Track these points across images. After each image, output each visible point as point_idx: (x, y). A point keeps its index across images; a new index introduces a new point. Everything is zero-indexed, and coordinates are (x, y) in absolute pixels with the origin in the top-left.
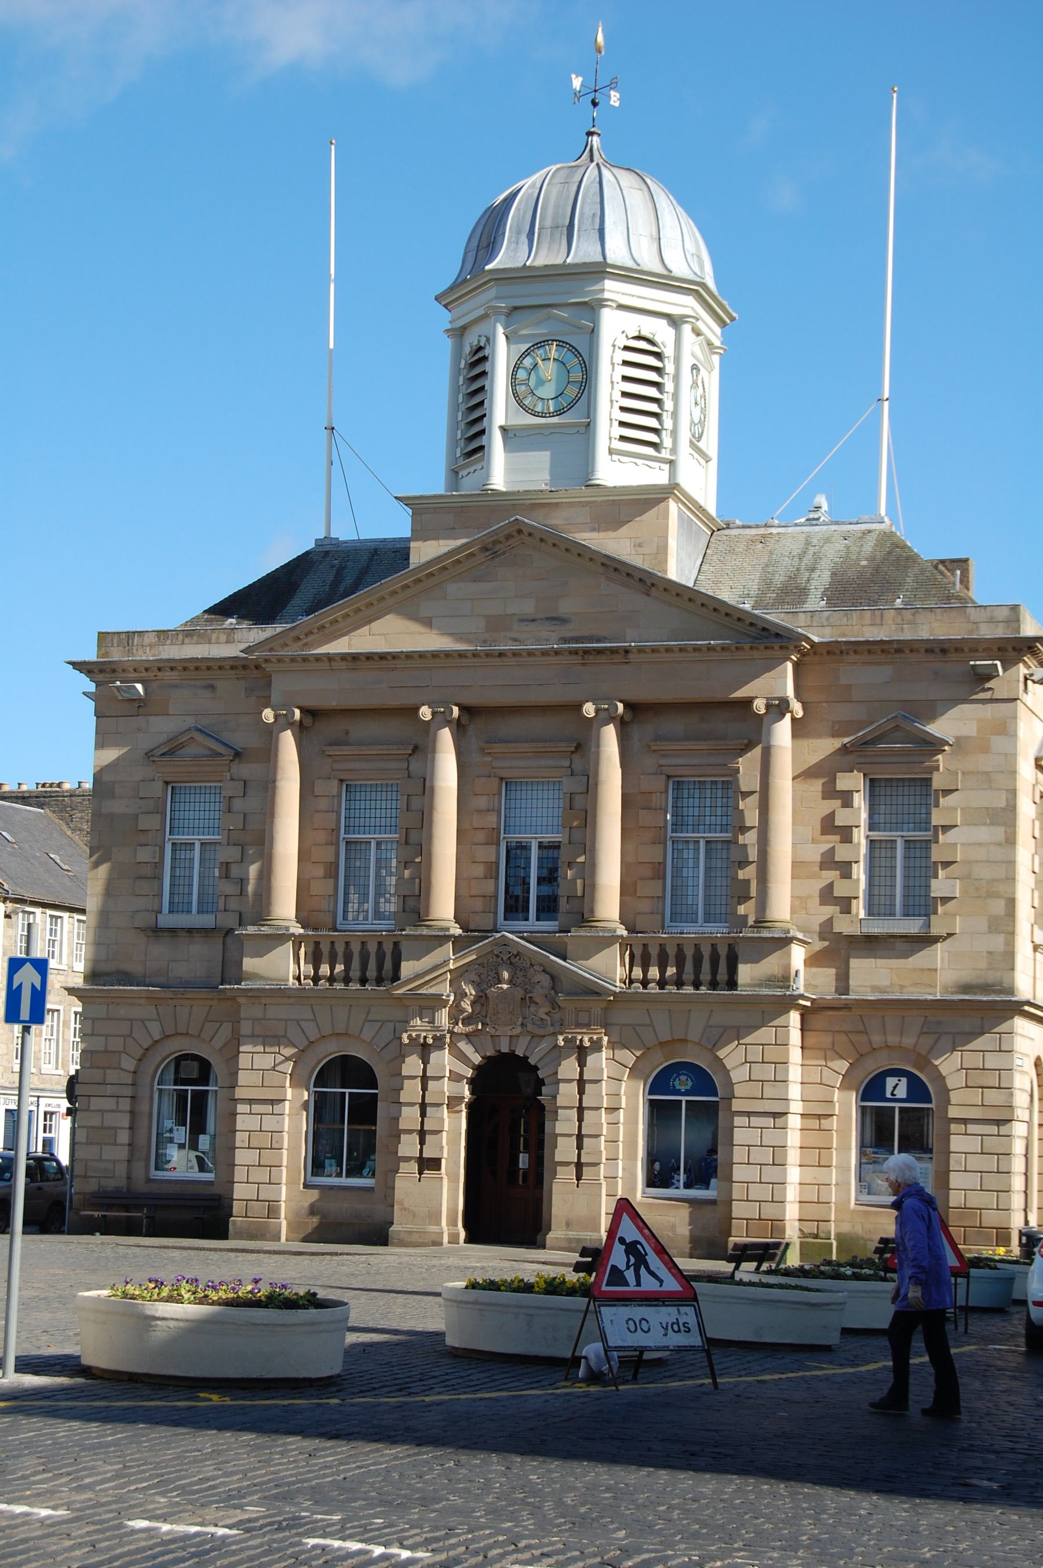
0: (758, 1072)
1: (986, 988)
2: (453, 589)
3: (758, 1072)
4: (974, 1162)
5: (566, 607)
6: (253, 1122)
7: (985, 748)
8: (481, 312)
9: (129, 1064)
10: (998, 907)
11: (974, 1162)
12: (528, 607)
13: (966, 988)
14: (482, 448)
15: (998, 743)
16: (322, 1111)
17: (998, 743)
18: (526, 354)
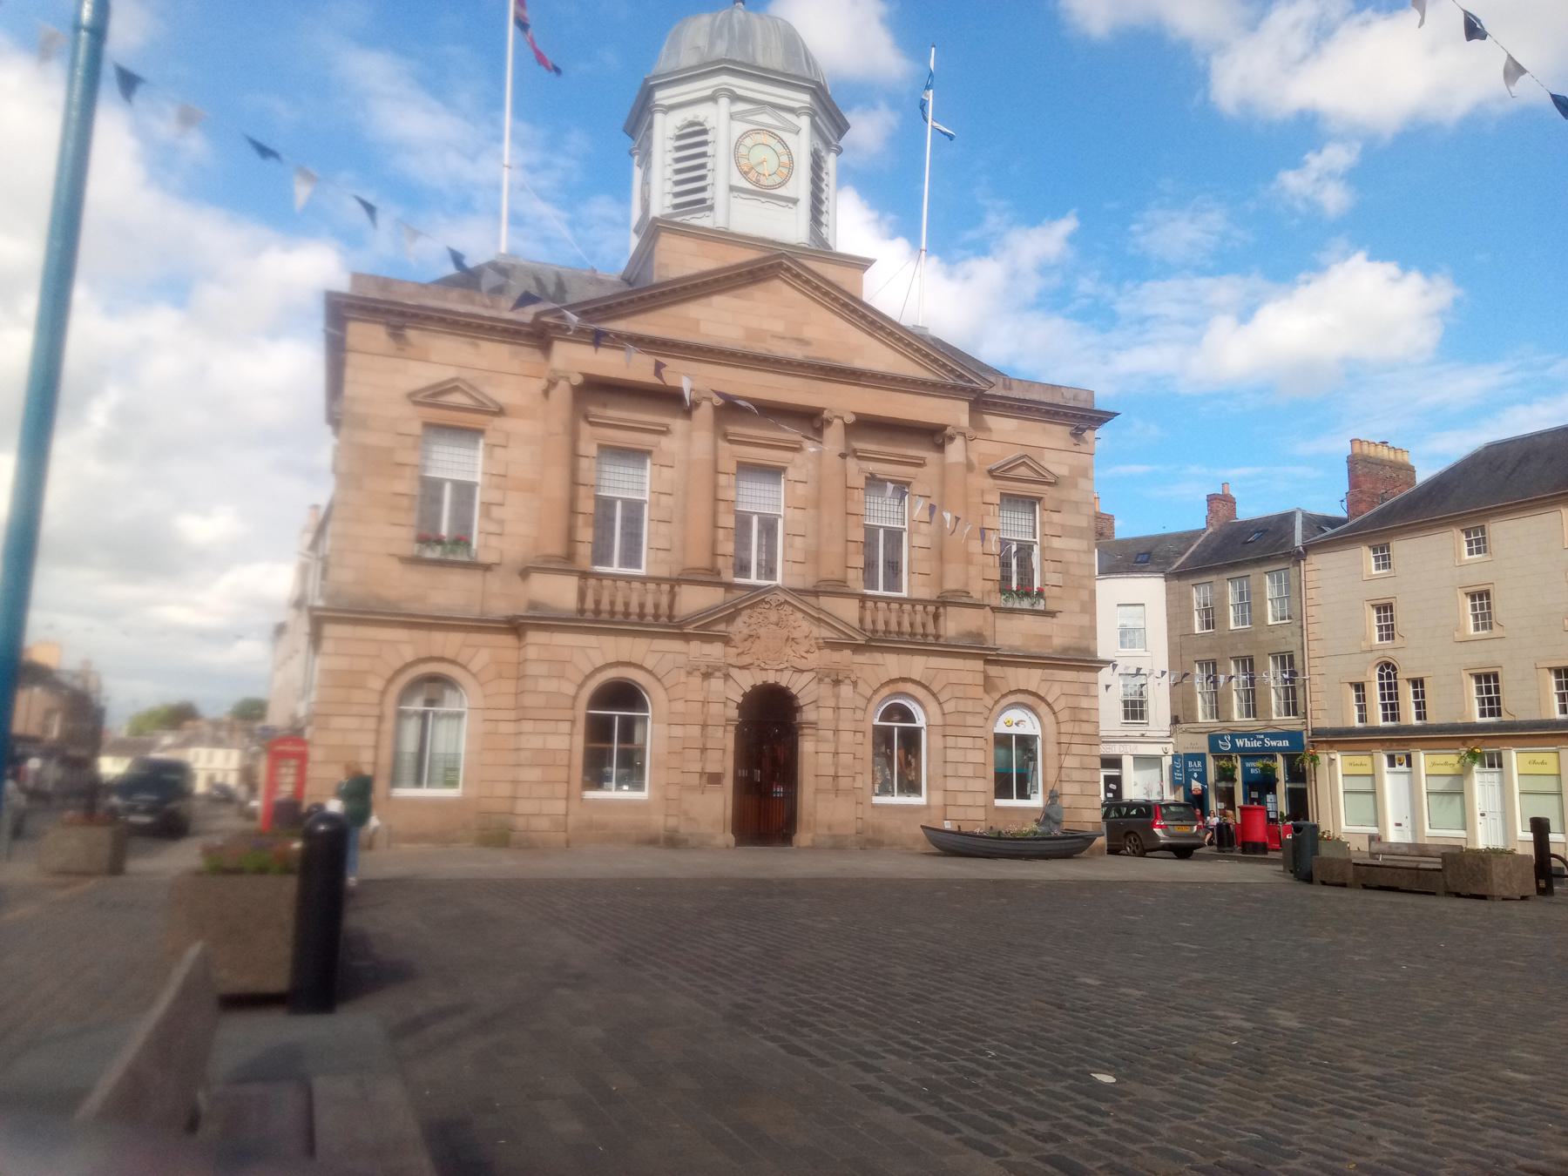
0: (962, 705)
1: (1078, 650)
2: (719, 300)
3: (962, 705)
4: (1076, 775)
5: (808, 333)
6: (536, 742)
7: (1075, 486)
8: (708, 92)
9: (377, 684)
10: (1085, 595)
11: (1076, 775)
12: (779, 327)
13: (1066, 650)
14: (703, 201)
15: (1082, 483)
16: (598, 730)
17: (1082, 483)
18: (746, 134)
